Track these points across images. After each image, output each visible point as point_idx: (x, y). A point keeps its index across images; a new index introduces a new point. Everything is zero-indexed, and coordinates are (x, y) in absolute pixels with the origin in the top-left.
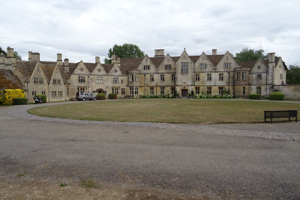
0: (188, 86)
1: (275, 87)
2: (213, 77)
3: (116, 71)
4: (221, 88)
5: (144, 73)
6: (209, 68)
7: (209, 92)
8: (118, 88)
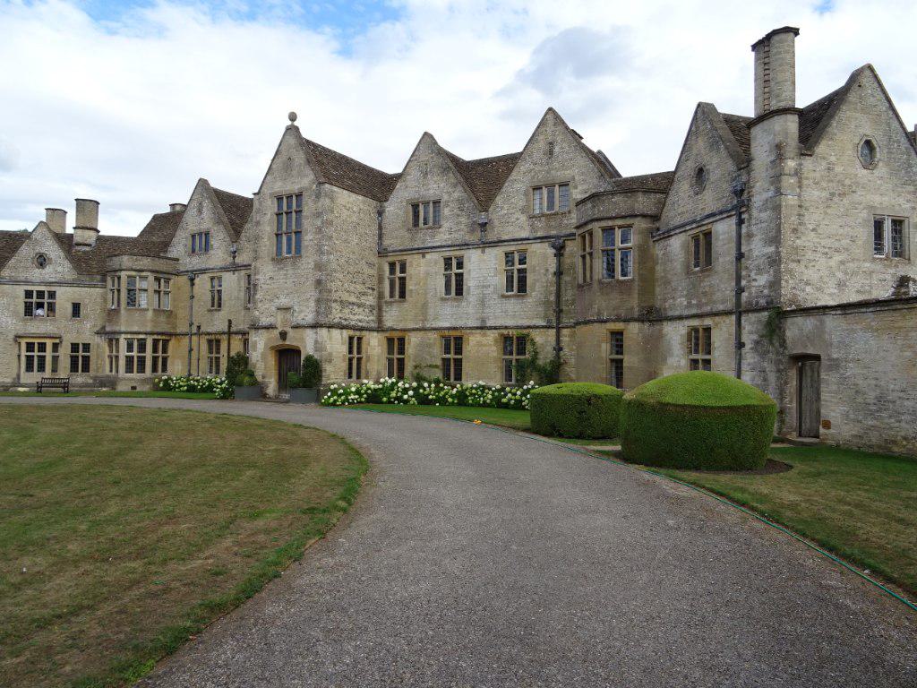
0: (296, 327)
1: (796, 330)
2: (473, 274)
3: (42, 261)
4: (515, 342)
5: (189, 267)
6: (452, 228)
7: (453, 368)
8: (42, 341)
